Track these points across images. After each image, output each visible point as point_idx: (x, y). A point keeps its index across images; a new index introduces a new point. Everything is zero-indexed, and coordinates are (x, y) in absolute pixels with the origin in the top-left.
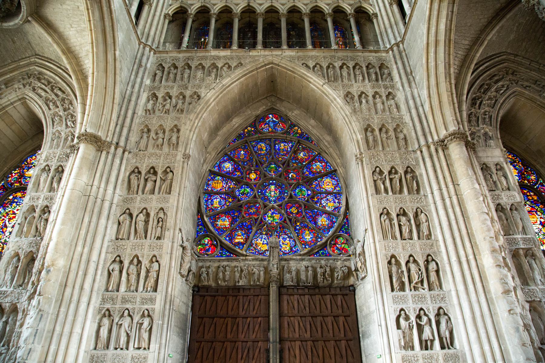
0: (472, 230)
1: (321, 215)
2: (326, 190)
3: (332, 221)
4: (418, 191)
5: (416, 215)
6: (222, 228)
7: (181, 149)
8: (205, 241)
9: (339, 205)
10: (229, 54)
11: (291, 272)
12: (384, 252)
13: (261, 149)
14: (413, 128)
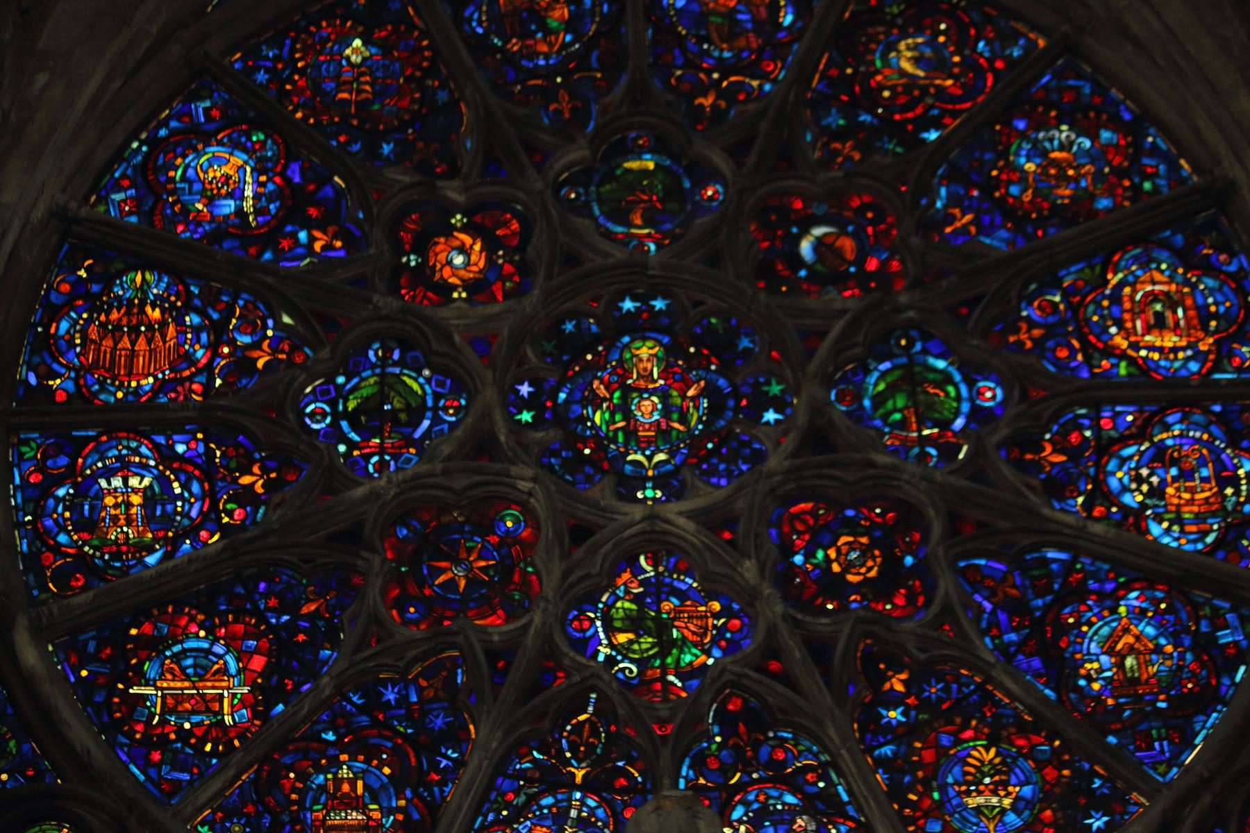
3: (1205, 646)
6: (183, 735)
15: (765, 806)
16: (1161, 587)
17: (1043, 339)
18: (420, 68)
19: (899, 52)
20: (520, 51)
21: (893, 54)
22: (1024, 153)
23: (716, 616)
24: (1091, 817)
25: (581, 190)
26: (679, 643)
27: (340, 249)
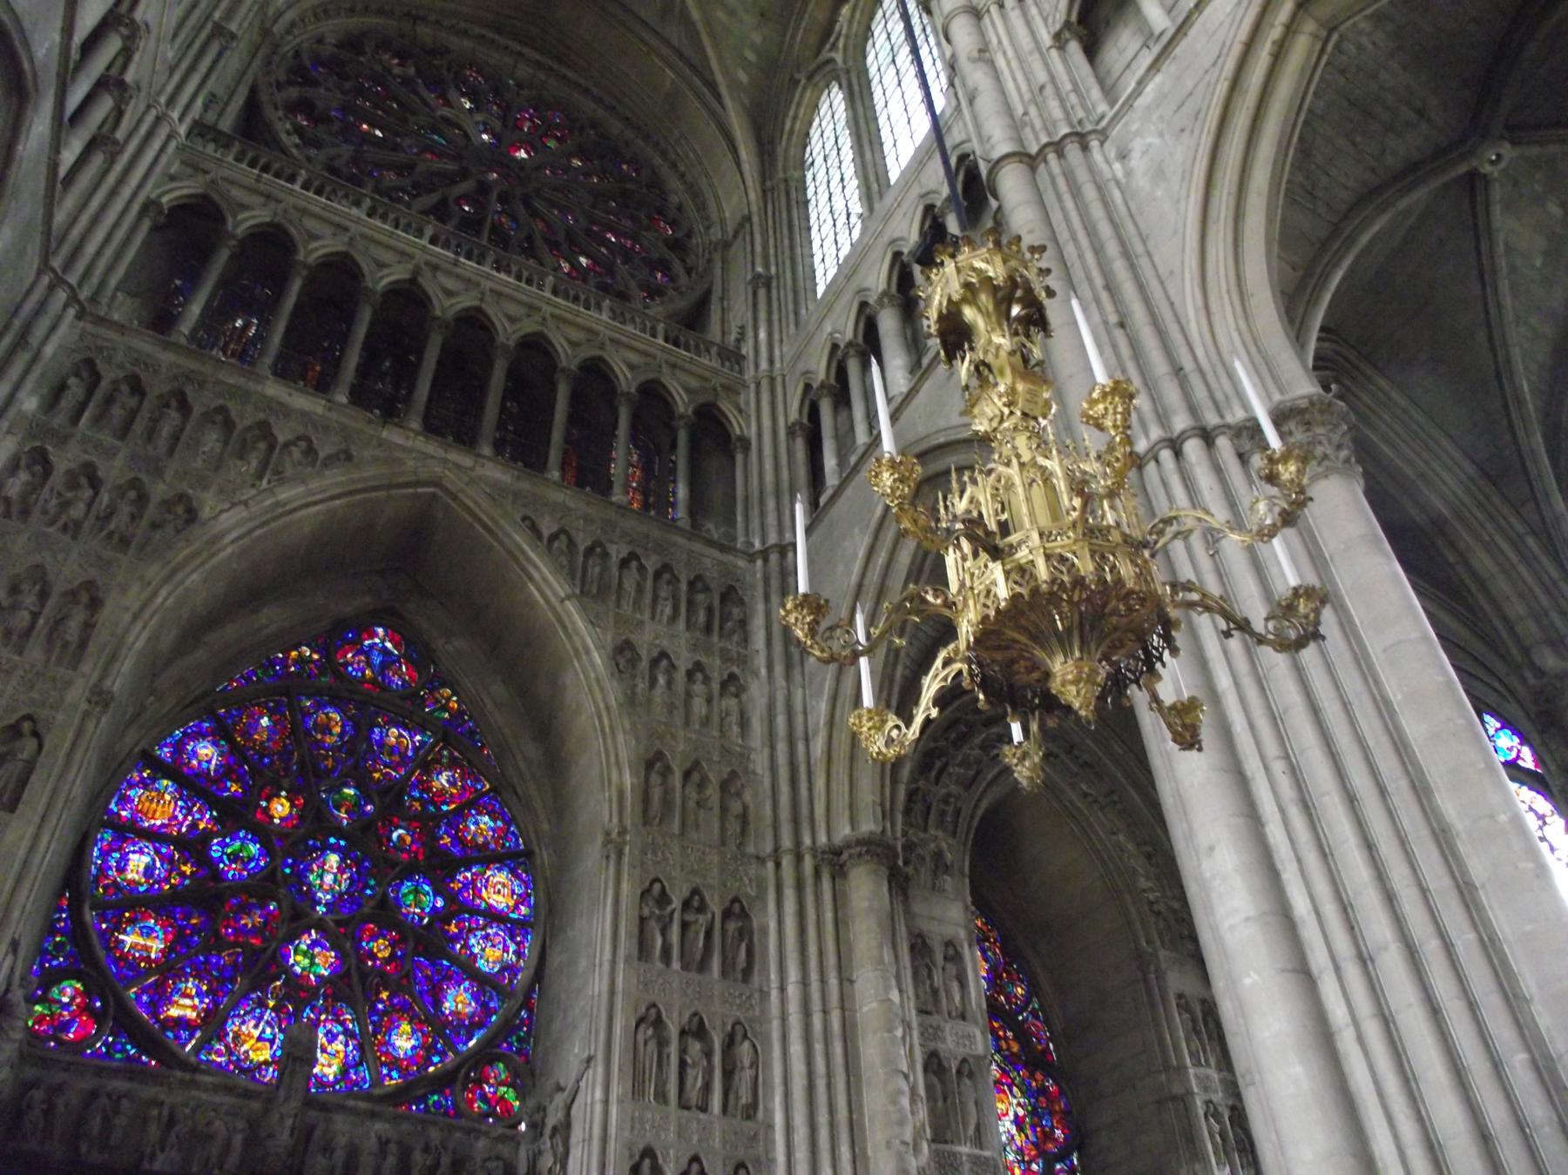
0: (861, 1114)
4: (747, 972)
5: (730, 1044)
7: (89, 668)
8: (62, 992)
9: (518, 961)
10: (320, 410)
11: (333, 1151)
12: (627, 1134)
13: (327, 730)
14: (769, 793)
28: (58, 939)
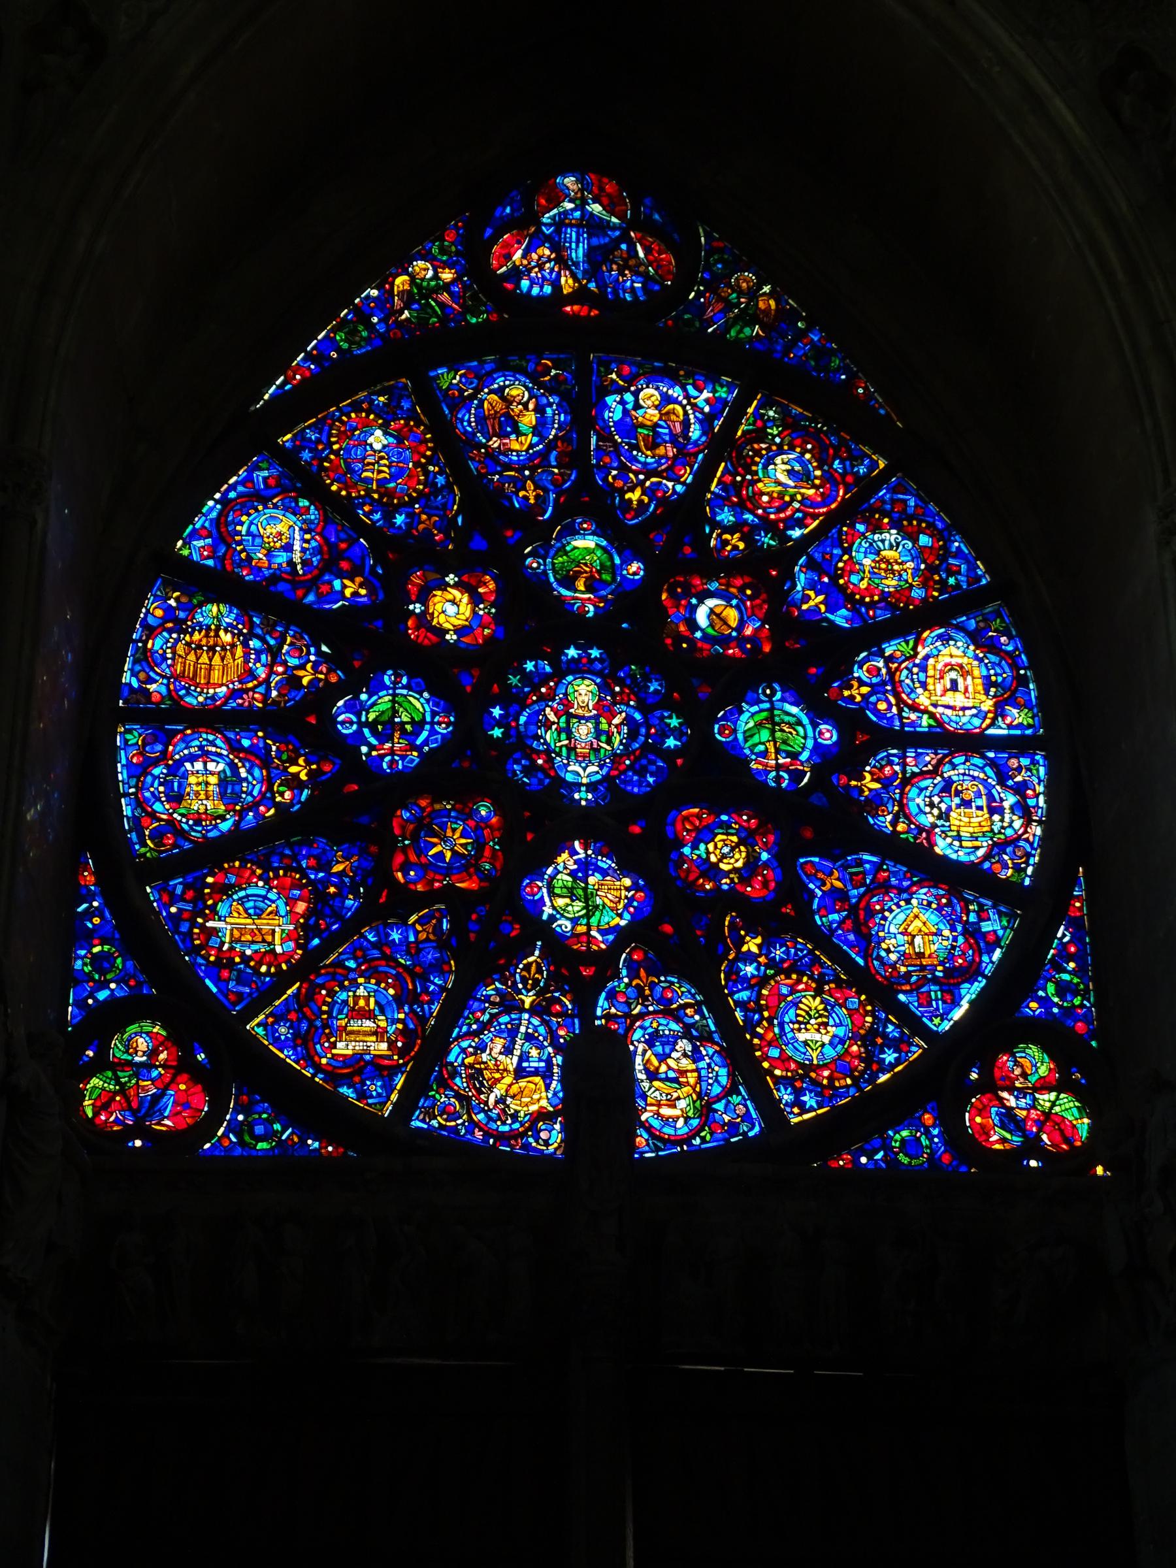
1: (906, 893)
2: (940, 723)
3: (972, 933)
6: (245, 959)
8: (128, 1047)
13: (508, 424)
15: (657, 1030)
16: (943, 886)
17: (870, 694)
18: (425, 457)
19: (776, 465)
20: (499, 447)
21: (772, 467)
22: (862, 550)
23: (628, 889)
24: (884, 1053)
25: (541, 561)
26: (601, 907)
27: (364, 596)
28: (96, 950)
